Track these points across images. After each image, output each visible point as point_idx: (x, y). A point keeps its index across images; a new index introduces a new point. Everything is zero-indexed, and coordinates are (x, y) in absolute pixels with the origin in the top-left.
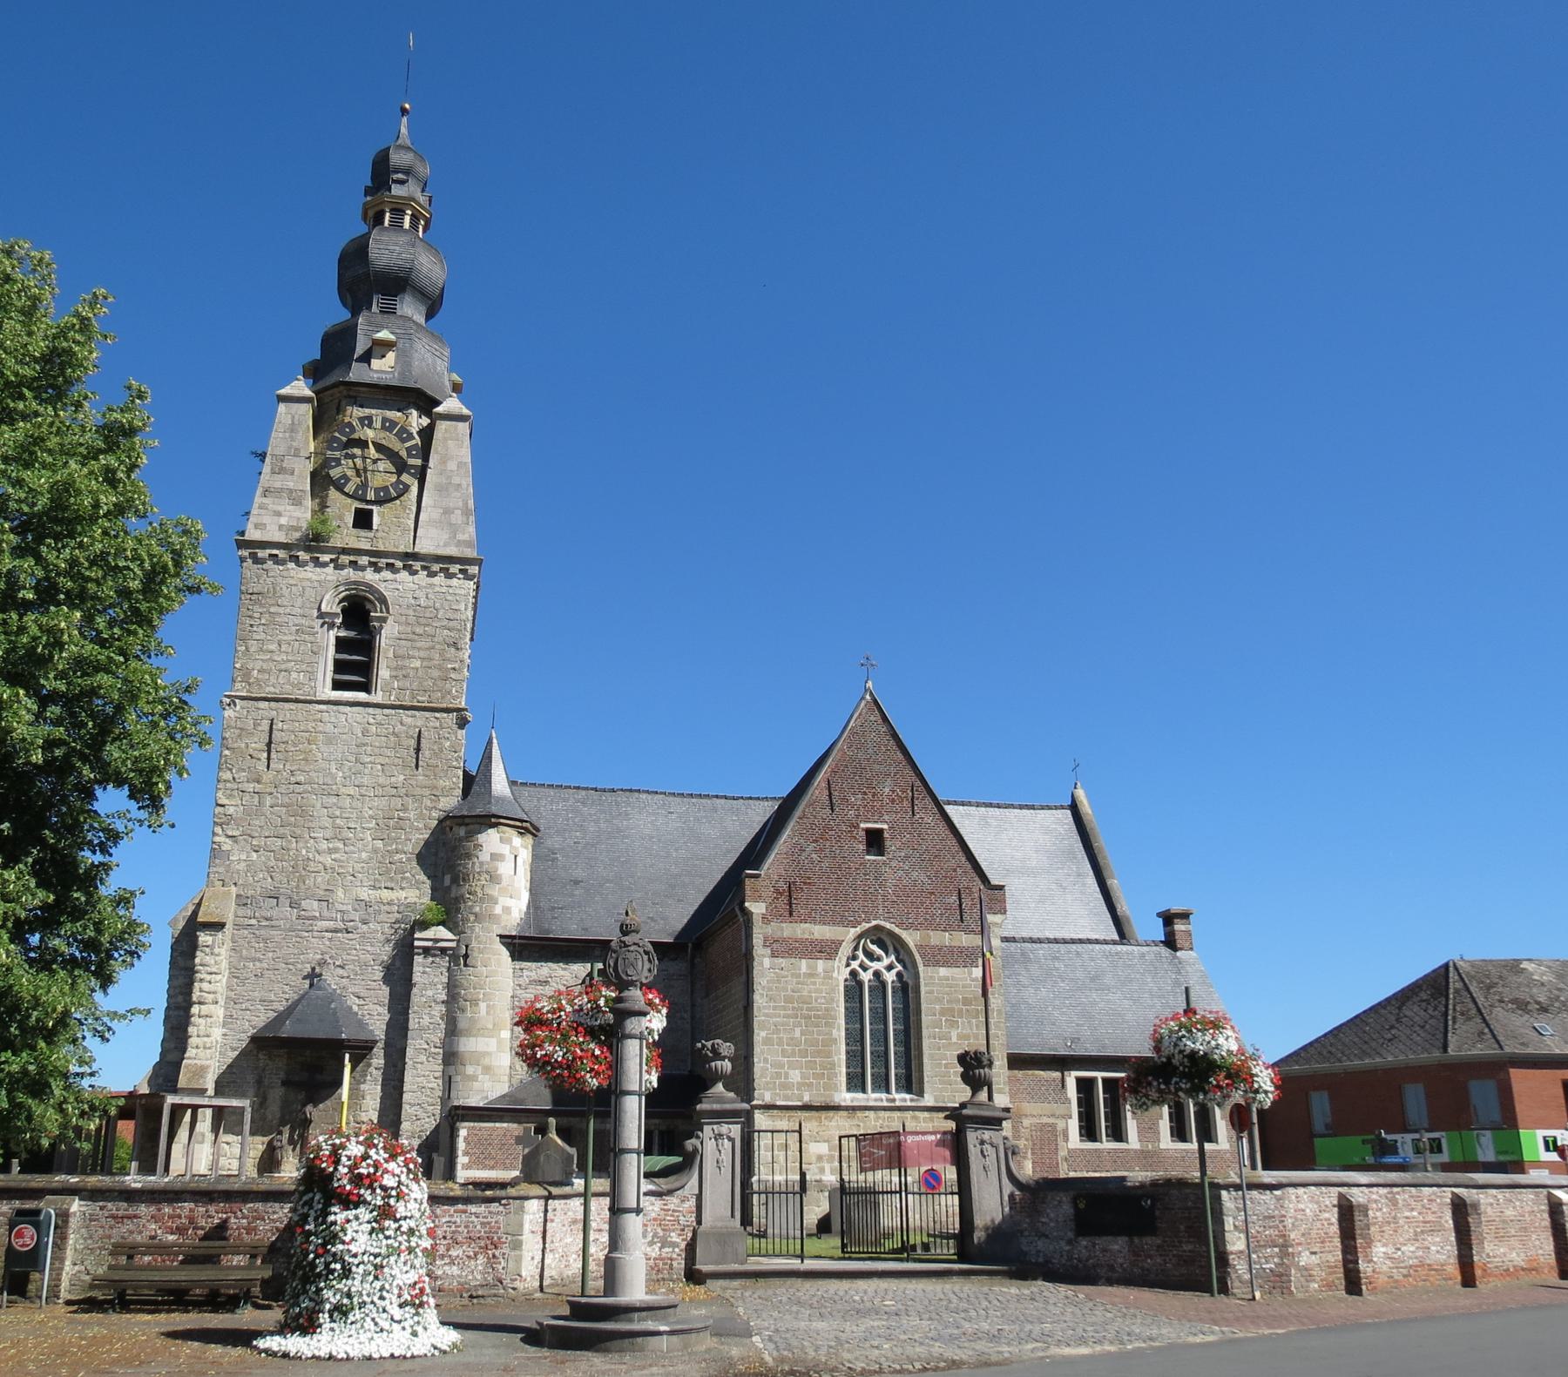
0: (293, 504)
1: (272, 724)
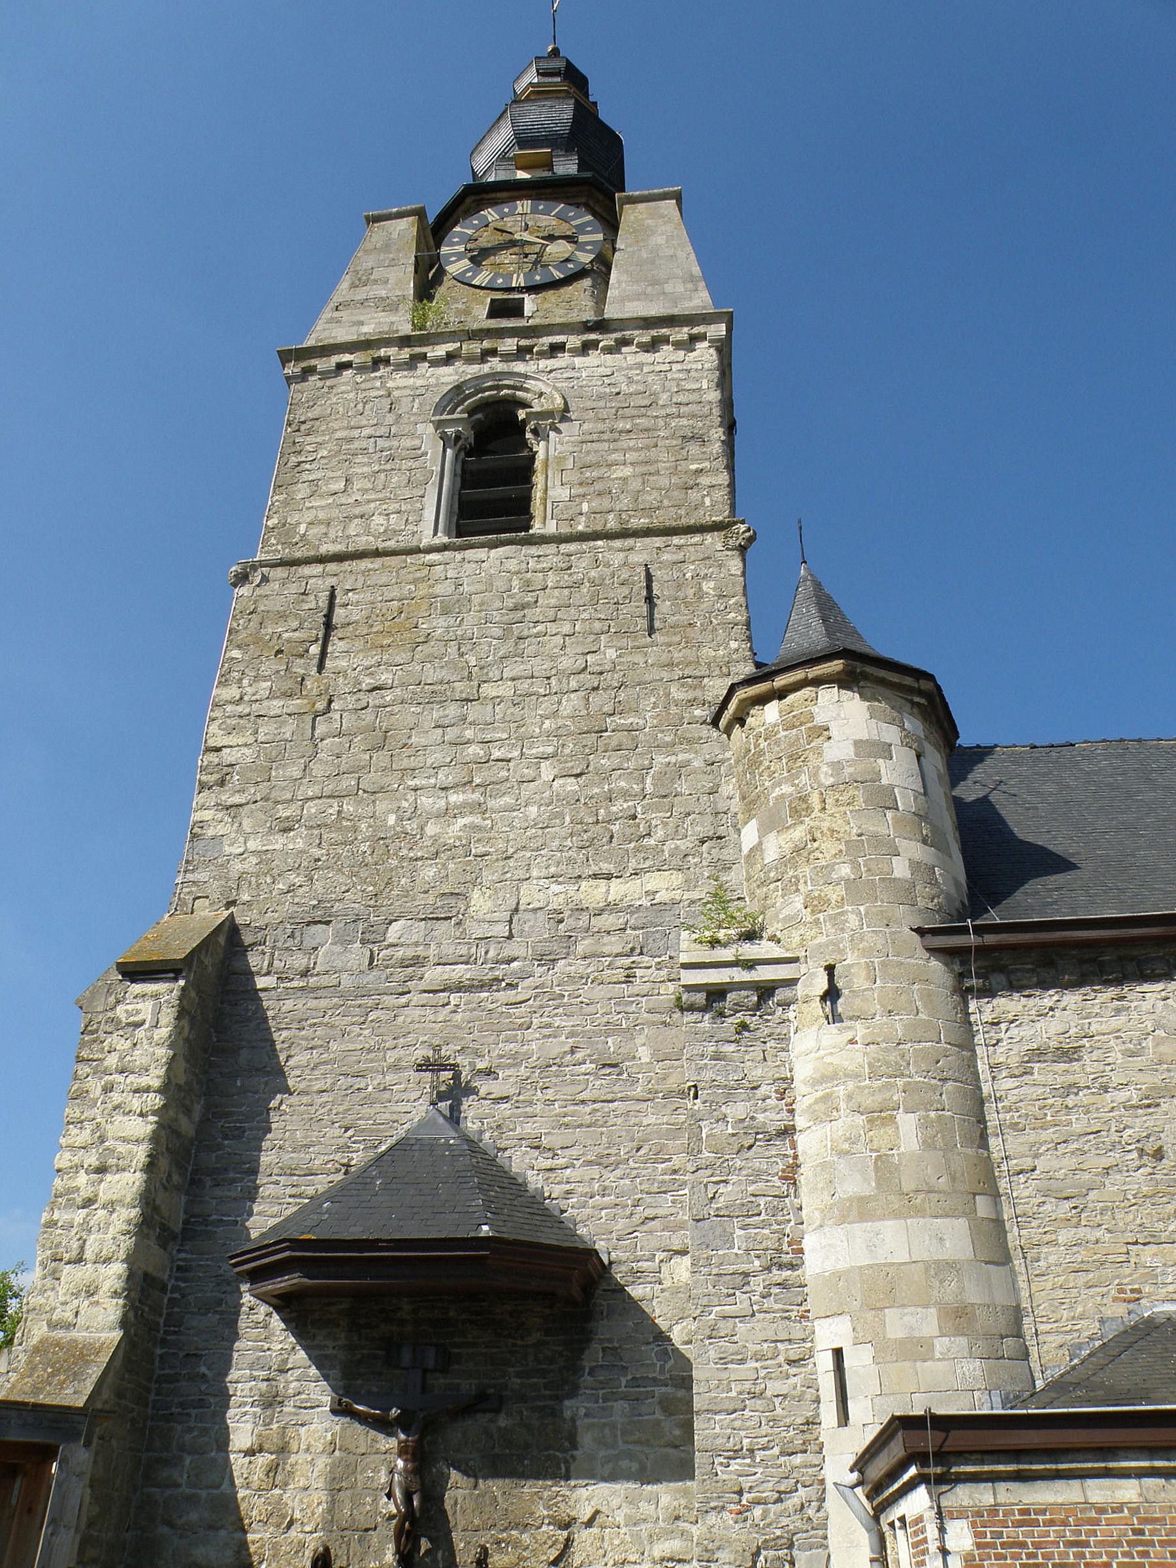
0: (383, 311)
1: (332, 597)
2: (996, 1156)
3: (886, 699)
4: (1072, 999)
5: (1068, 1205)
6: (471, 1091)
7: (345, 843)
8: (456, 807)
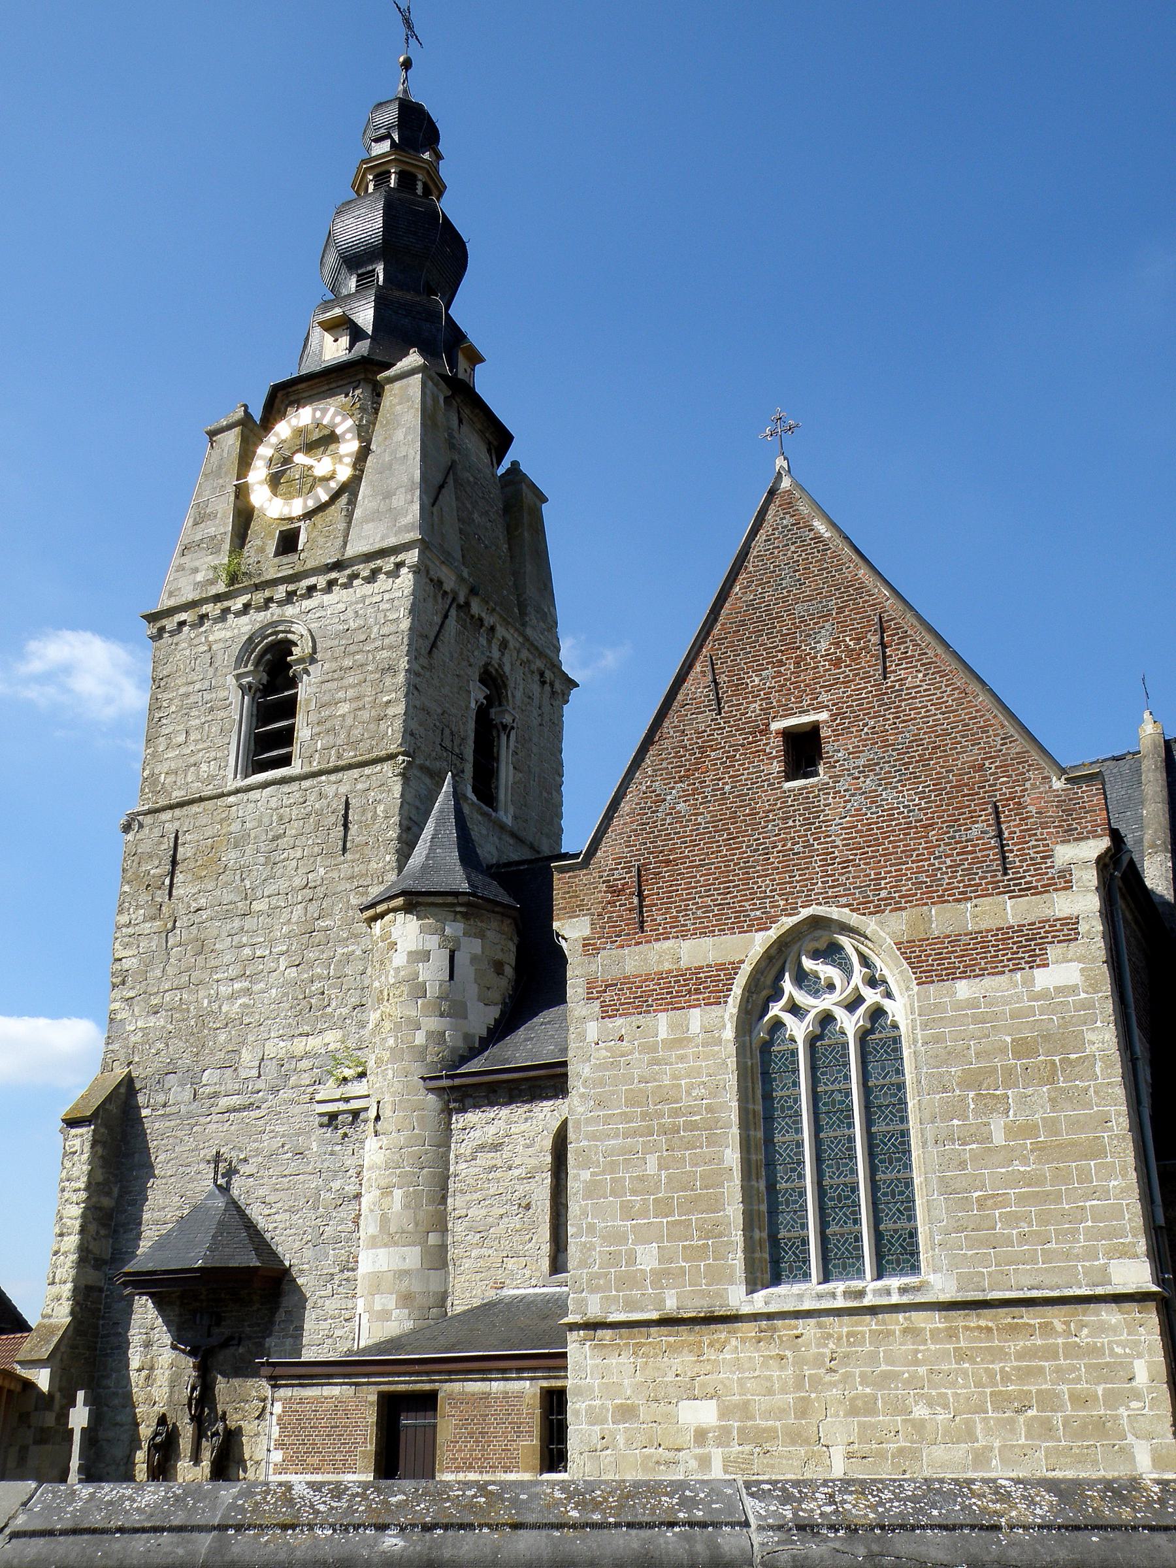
0: (212, 554)
1: (176, 838)
2: (450, 1208)
3: (434, 916)
4: (505, 1112)
5: (479, 1235)
6: (236, 1172)
7: (183, 1020)
8: (238, 992)
